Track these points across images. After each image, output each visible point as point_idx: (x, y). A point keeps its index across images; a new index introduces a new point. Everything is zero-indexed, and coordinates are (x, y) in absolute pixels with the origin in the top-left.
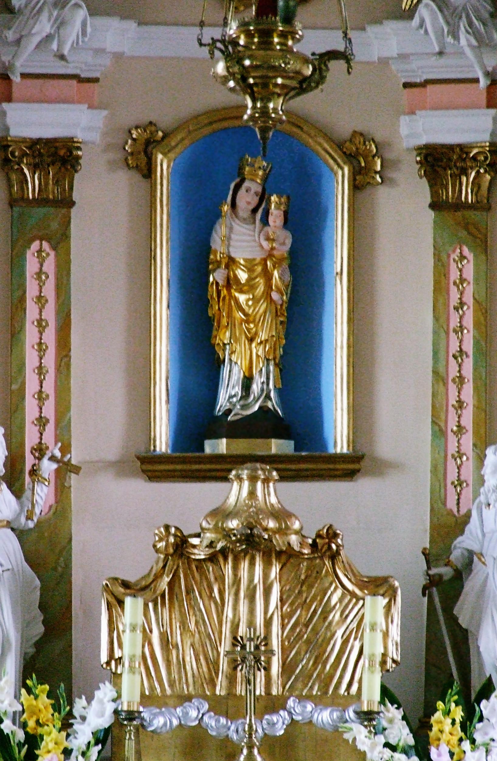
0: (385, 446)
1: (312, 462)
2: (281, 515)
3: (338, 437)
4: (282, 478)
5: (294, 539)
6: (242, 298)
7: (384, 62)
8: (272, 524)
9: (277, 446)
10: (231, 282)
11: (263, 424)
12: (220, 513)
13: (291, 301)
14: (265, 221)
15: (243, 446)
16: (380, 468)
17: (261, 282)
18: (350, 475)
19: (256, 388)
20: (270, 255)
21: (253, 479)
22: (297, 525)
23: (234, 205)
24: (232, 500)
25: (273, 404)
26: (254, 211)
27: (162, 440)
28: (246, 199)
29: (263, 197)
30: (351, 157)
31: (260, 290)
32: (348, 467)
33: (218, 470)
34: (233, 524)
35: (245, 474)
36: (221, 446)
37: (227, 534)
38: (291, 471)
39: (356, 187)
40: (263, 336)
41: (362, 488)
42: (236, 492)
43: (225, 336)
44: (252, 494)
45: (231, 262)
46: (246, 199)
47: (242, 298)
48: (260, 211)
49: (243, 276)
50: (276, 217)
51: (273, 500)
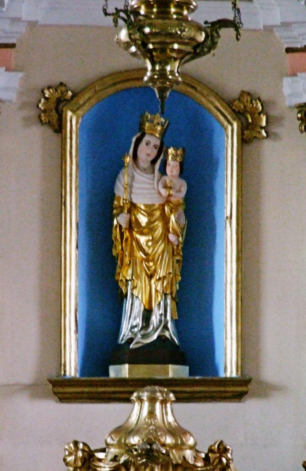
0: (269, 371)
1: (205, 385)
2: (178, 432)
3: (228, 363)
4: (179, 400)
5: (189, 454)
6: (143, 239)
7: (269, 29)
8: (169, 440)
9: (174, 371)
10: (133, 225)
11: (161, 352)
12: (123, 431)
13: (186, 242)
14: (163, 171)
15: (143, 371)
16: (266, 390)
17: (159, 225)
18: (239, 397)
19: (155, 319)
20: (168, 201)
21: (152, 400)
22: (191, 442)
23: (135, 157)
24: (134, 419)
25: (171, 333)
26: (154, 162)
27: (72, 366)
28: (146, 152)
29: (161, 150)
30: (239, 114)
31: (159, 232)
32: (236, 390)
33: (122, 393)
34: (135, 440)
35: (145, 396)
36: (123, 371)
37: (129, 449)
38: (185, 393)
39: (244, 141)
40: (161, 273)
41: (249, 407)
42: (137, 412)
43: (128, 273)
44: (151, 413)
45: (133, 207)
46: (146, 152)
47: (143, 239)
48: (159, 162)
49: (143, 220)
50: (173, 167)
51: (170, 419)
